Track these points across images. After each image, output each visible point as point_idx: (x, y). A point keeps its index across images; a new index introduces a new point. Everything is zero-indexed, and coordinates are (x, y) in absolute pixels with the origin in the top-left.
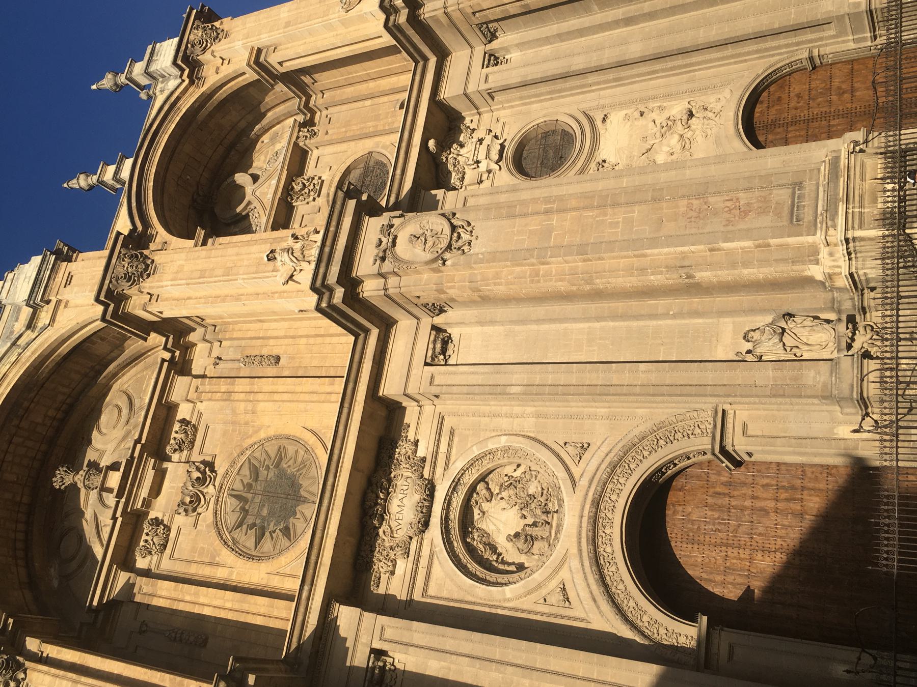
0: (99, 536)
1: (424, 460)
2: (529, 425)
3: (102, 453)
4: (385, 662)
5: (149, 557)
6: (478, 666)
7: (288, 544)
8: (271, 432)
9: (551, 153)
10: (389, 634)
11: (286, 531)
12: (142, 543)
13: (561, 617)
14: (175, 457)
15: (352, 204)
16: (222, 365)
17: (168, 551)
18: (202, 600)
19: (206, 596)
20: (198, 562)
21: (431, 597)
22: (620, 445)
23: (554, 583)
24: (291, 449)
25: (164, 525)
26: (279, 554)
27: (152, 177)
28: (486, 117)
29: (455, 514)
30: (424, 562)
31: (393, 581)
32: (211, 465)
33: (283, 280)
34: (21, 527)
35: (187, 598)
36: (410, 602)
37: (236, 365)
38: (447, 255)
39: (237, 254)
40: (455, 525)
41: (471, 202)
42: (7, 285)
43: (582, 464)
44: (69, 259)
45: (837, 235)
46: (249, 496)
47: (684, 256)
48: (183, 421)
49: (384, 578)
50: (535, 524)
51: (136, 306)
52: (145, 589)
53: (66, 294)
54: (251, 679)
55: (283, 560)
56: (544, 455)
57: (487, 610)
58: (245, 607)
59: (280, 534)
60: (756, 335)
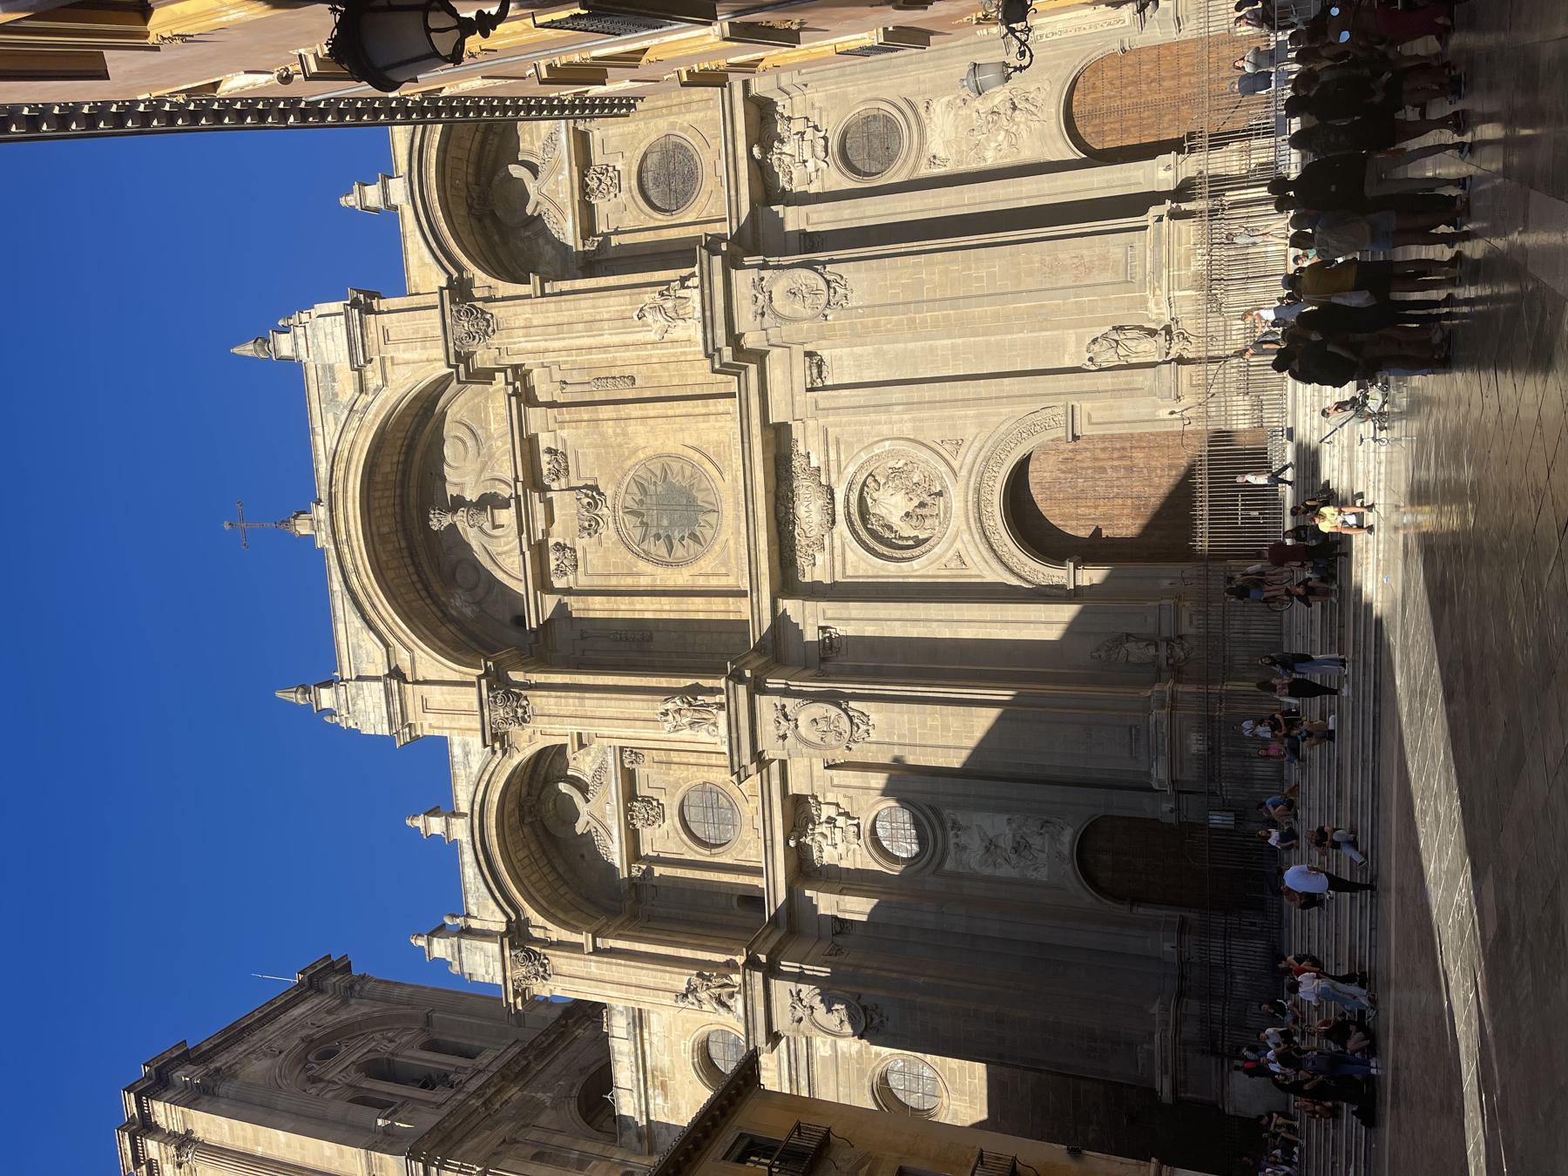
1: (818, 469)
2: (907, 430)
3: (461, 485)
8: (650, 452)
9: (876, 143)
10: (829, 614)
11: (693, 537)
12: (553, 567)
14: (555, 486)
15: (717, 261)
16: (569, 389)
17: (581, 569)
18: (638, 607)
22: (990, 442)
23: (951, 553)
24: (676, 466)
27: (437, 205)
28: (798, 99)
29: (854, 509)
30: (838, 551)
32: (595, 488)
33: (657, 338)
34: (411, 569)
37: (587, 388)
38: (827, 312)
39: (594, 307)
40: (856, 517)
41: (814, 218)
42: (301, 341)
43: (960, 458)
44: (370, 310)
45: (1164, 299)
46: (643, 510)
47: (1042, 306)
48: (549, 451)
50: (922, 505)
51: (483, 357)
52: (576, 606)
53: (390, 351)
54: (748, 673)
55: (702, 562)
56: (925, 454)
58: (684, 607)
60: (1096, 348)
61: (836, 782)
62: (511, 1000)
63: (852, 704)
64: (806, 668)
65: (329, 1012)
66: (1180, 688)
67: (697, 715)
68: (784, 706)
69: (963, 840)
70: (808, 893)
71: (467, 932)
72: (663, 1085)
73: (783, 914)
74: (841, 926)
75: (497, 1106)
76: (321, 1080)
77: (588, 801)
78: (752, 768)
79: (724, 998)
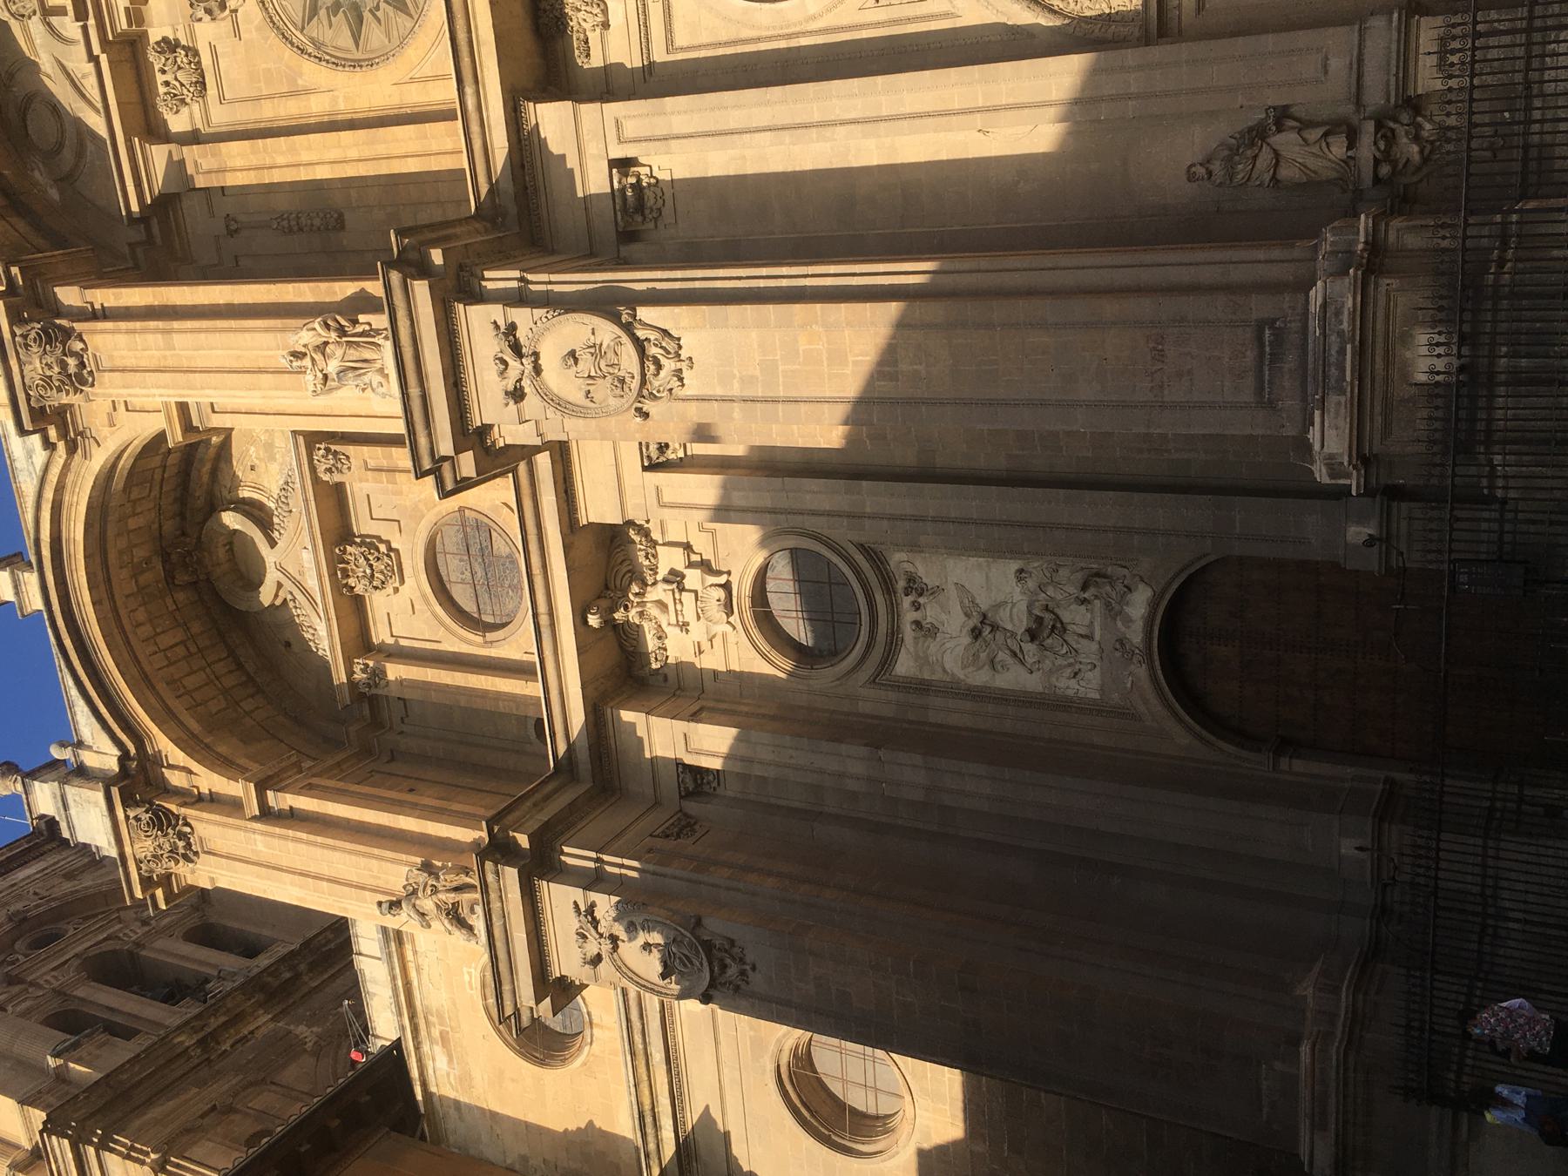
0: (83, 96)
4: (638, 176)
5: (185, 110)
6: (787, 140)
7: (409, 24)
10: (630, 130)
12: (162, 90)
13: (909, 20)
17: (212, 91)
18: (305, 157)
19: (309, 148)
20: (270, 97)
21: (682, 49)
25: (184, 48)
26: (401, 45)
31: (609, 41)
35: (281, 160)
36: (650, 69)
49: (594, 38)
52: (205, 167)
54: (437, 256)
55: (412, 53)
57: (783, 44)
58: (381, 150)
59: (390, 9)
61: (666, 499)
62: (139, 894)
63: (644, 313)
64: (592, 255)
65: (70, 876)
66: (1396, 223)
67: (354, 354)
68: (512, 328)
69: (931, 613)
70: (627, 716)
71: (82, 773)
72: (444, 1039)
73: (583, 756)
74: (695, 780)
75: (226, 1046)
76: (20, 981)
77: (273, 543)
78: (467, 464)
79: (464, 912)
